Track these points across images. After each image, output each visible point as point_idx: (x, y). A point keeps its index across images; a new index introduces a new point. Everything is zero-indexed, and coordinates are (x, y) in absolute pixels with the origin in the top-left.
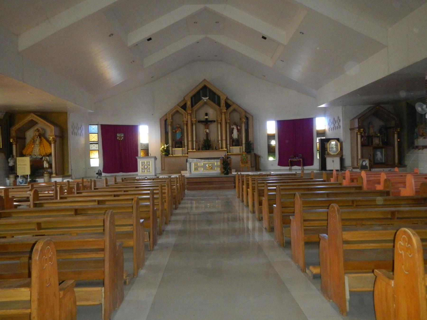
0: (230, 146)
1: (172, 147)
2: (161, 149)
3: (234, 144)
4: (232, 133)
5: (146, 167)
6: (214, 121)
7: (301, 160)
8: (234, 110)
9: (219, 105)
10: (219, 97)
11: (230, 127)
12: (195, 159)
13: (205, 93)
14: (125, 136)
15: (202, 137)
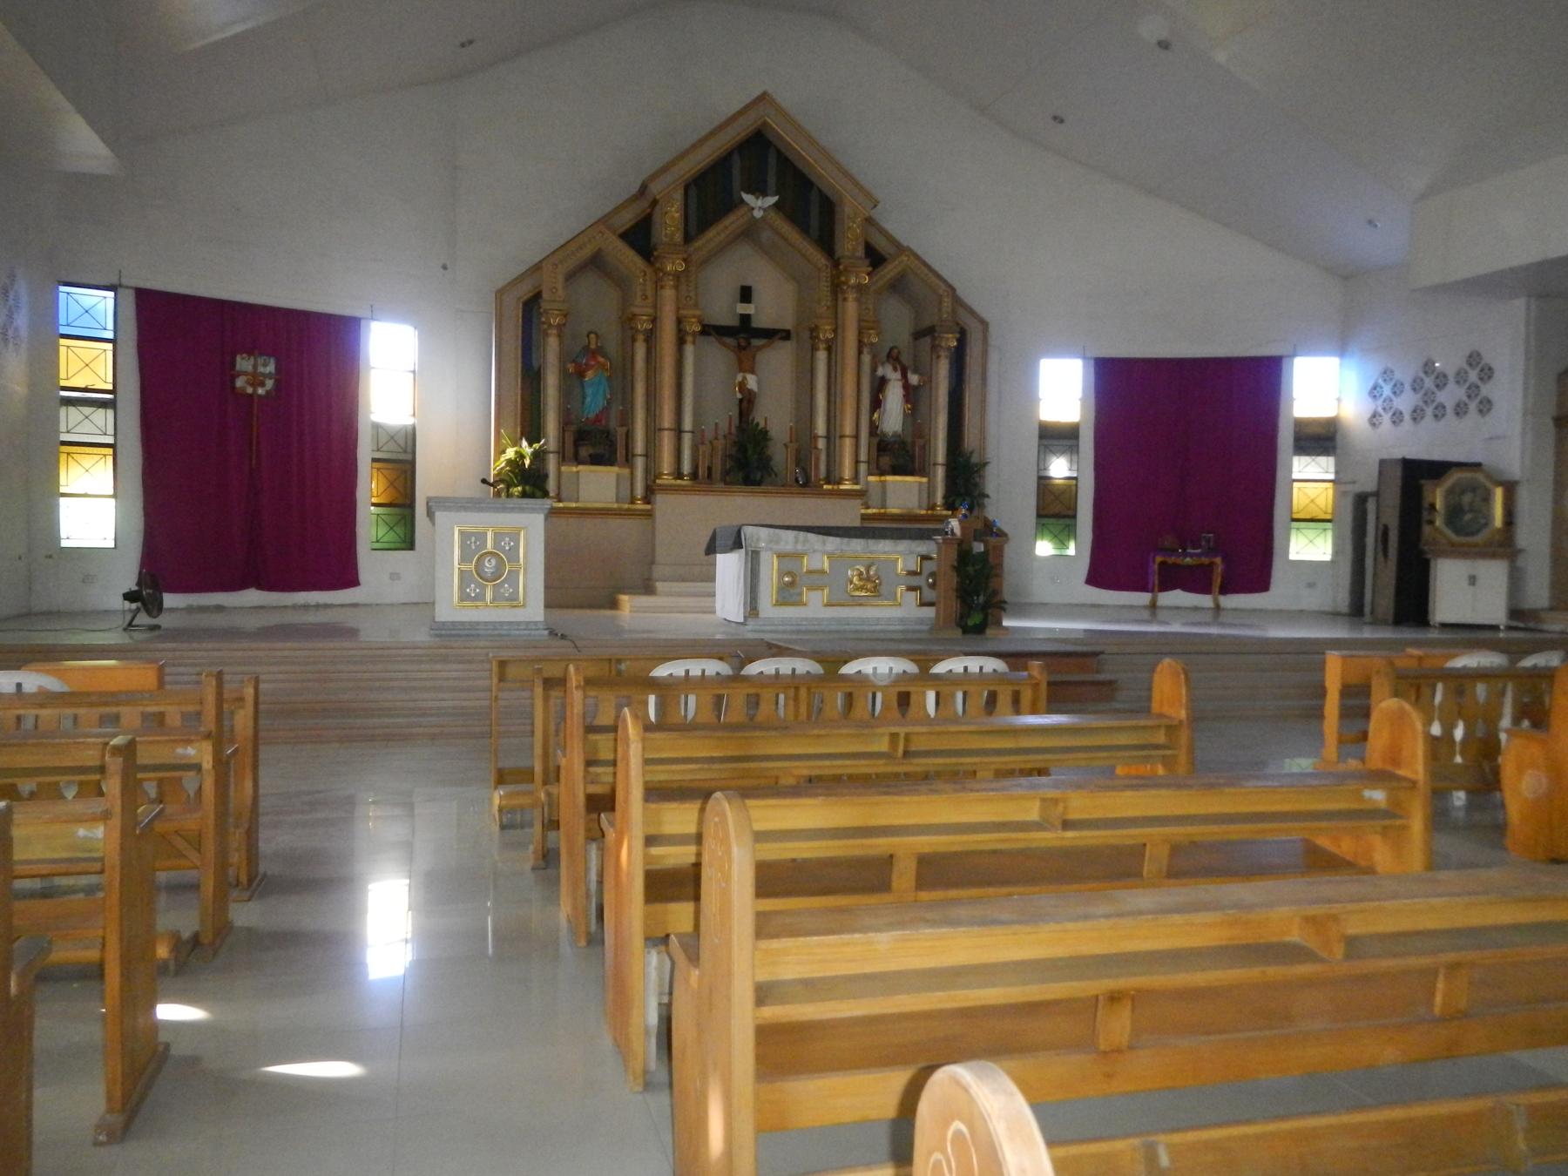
1: (563, 458)
2: (502, 462)
4: (876, 404)
5: (489, 565)
6: (786, 335)
7: (1218, 560)
8: (898, 286)
10: (829, 207)
11: (874, 370)
12: (791, 534)
13: (757, 173)
14: (282, 377)
15: (722, 416)
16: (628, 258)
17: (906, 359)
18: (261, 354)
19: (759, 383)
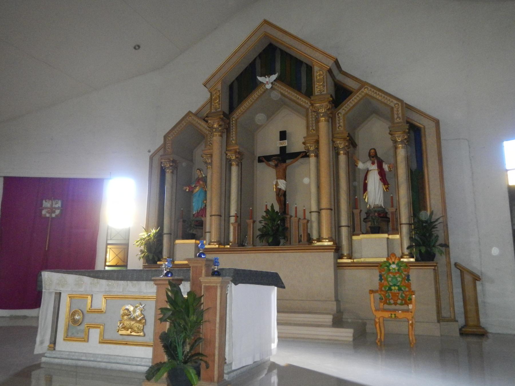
6: (305, 155)
14: (64, 208)
18: (54, 199)
19: (287, 185)
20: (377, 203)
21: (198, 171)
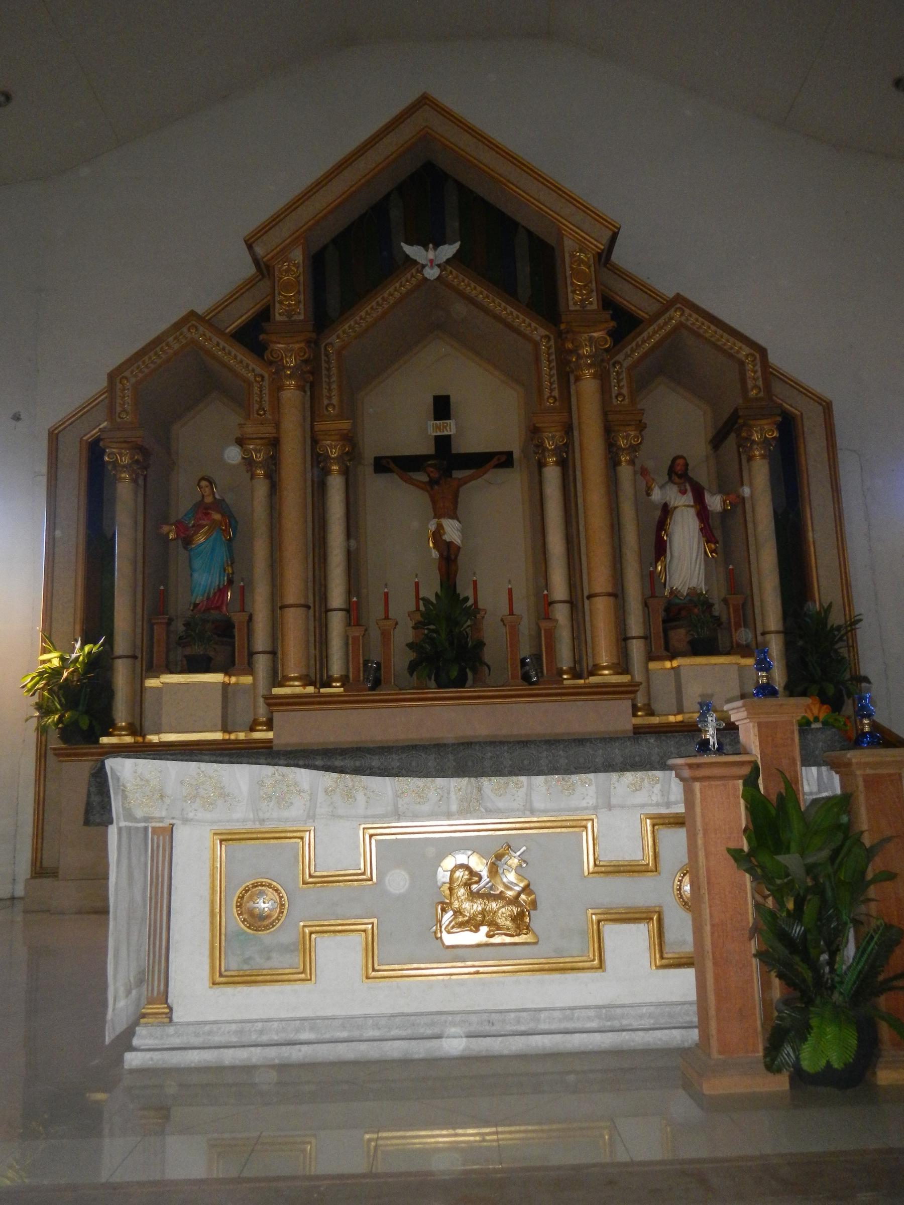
0: (651, 657)
3: (680, 636)
4: (660, 549)
6: (505, 460)
8: (669, 366)
9: (546, 304)
10: (545, 255)
16: (238, 359)
17: (702, 474)
19: (463, 532)
20: (694, 583)
21: (204, 483)
